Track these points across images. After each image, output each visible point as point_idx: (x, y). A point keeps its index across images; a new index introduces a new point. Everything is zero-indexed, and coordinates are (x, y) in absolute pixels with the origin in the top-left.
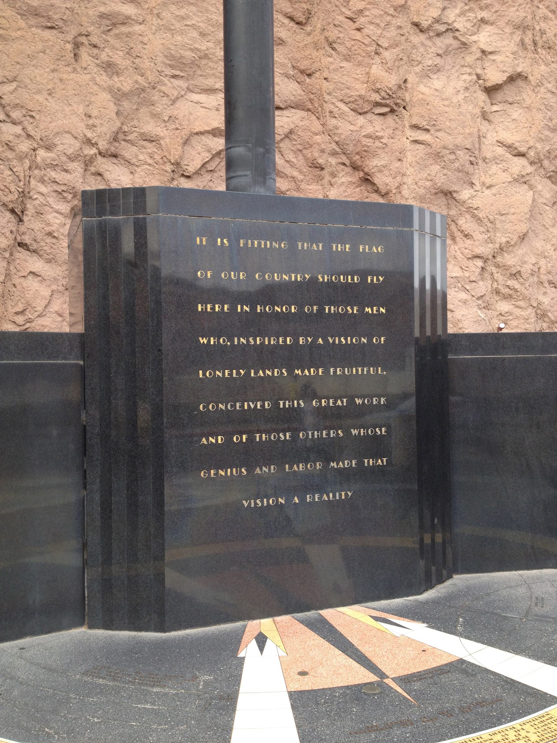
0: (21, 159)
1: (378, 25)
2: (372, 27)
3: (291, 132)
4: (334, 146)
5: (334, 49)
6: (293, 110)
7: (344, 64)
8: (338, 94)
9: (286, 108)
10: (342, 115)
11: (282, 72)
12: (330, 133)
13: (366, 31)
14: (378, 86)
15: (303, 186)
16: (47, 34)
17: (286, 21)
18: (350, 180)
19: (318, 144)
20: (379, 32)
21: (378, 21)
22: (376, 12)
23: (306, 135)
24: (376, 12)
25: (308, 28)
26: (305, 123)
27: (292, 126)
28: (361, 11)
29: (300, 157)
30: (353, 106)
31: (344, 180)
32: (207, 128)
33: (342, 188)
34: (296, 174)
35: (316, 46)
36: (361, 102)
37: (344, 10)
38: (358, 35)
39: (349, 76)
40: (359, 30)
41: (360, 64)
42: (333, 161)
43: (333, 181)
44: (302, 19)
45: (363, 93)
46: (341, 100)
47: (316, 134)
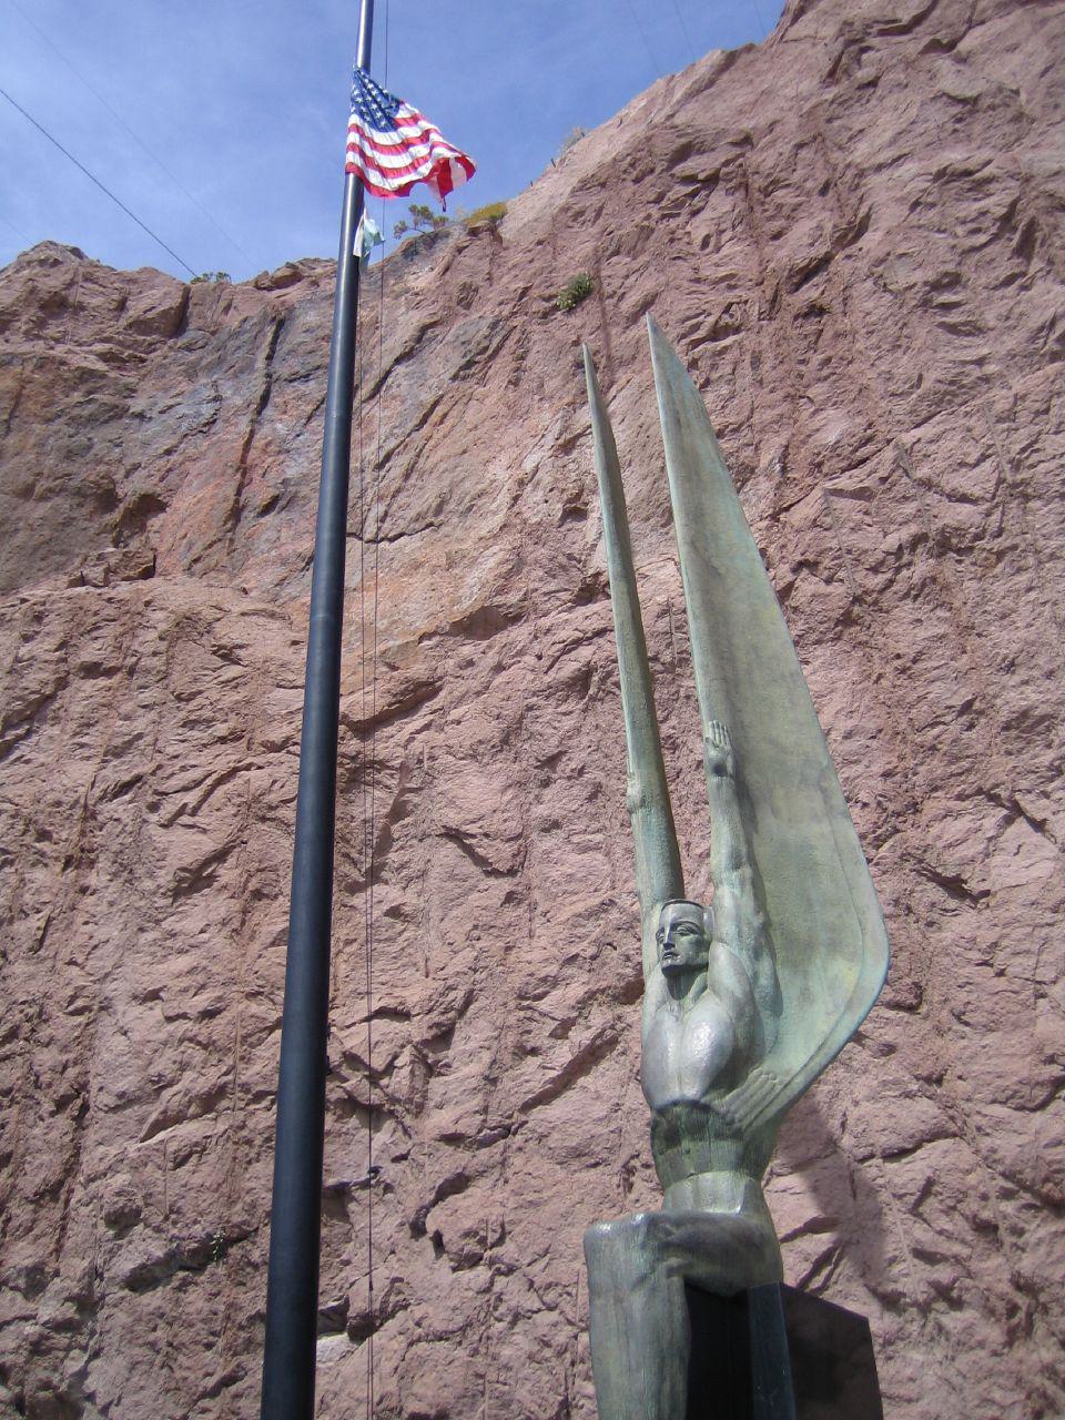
0: (560, 1354)
1: (1028, 952)
2: (1019, 960)
3: (930, 1183)
4: (1002, 1182)
5: (967, 1024)
6: (930, 1145)
7: (990, 1039)
8: (987, 1094)
9: (918, 1146)
10: (999, 1123)
11: (897, 1093)
12: (990, 1159)
13: (1010, 971)
14: (1049, 1051)
15: (974, 1265)
16: (592, 1174)
17: (891, 1014)
18: (1053, 1229)
19: (974, 1188)
20: (1032, 962)
21: (1026, 945)
22: (1019, 933)
23: (952, 1180)
24: (1019, 933)
25: (924, 1009)
26: (951, 1158)
27: (929, 1173)
28: (995, 945)
29: (957, 1216)
30: (1016, 1101)
31: (1042, 1232)
32: (798, 1225)
33: (1043, 1250)
34: (957, 1248)
35: (939, 1031)
36: (1026, 1090)
37: (970, 955)
38: (1002, 983)
39: (1000, 1055)
40: (1001, 973)
41: (1016, 1026)
42: (1008, 1207)
43: (1020, 1242)
44: (911, 1000)
45: (1025, 1073)
46: (994, 1101)
47: (968, 1172)
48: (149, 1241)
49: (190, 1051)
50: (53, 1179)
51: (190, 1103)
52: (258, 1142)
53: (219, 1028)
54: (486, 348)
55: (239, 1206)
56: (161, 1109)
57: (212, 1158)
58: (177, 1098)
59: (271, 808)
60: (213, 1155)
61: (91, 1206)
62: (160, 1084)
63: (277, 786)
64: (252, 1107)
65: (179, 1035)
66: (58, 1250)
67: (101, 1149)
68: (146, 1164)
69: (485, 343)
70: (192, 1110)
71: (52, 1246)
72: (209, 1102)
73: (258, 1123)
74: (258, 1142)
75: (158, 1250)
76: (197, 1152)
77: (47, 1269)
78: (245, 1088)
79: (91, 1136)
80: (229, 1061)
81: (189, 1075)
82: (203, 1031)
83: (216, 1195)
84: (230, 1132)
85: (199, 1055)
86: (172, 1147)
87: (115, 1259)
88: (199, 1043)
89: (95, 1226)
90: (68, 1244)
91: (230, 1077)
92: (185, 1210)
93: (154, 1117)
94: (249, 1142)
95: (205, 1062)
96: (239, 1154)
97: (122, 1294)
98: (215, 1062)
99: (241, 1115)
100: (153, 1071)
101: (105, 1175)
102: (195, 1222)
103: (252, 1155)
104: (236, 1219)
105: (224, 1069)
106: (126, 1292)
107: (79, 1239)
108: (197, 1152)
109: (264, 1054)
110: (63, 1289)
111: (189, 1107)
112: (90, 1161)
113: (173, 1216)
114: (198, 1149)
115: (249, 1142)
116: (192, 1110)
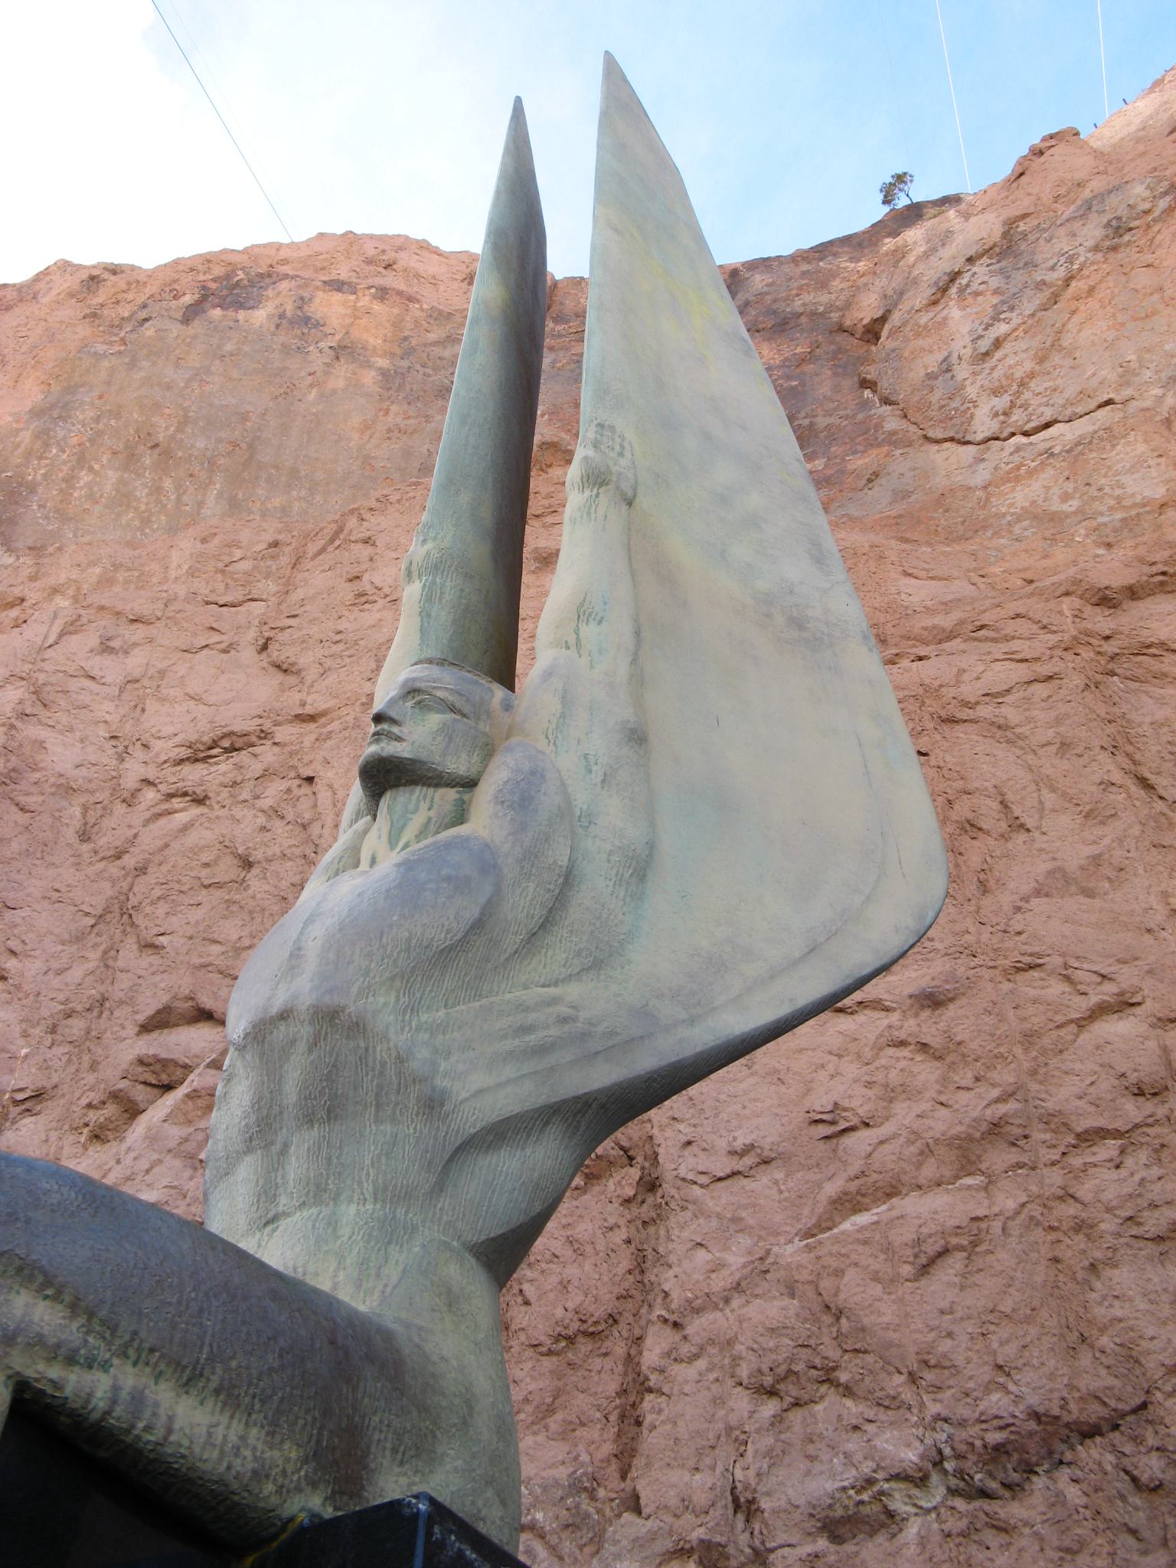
48: (870, 1428)
49: (903, 1064)
50: (599, 1312)
51: (927, 1151)
52: (1108, 1225)
53: (960, 1020)
54: (1146, 212)
55: (1085, 1359)
56: (854, 1170)
57: (1003, 1258)
58: (887, 1148)
59: (966, 704)
60: (1001, 1254)
61: (701, 1364)
62: (833, 1126)
63: (966, 677)
64: (1076, 1161)
65: (872, 1037)
66: (625, 1457)
67: (701, 1255)
68: (839, 1273)
69: (1147, 206)
70: (929, 1171)
71: (608, 1448)
72: (965, 1154)
73: (1099, 1190)
74: (1108, 1225)
75: (901, 1446)
76: (962, 1248)
77: (601, 1493)
78: (1056, 1121)
79: (680, 1233)
80: (1005, 1076)
81: (904, 1114)
82: (929, 1027)
83: (1033, 1331)
84: (1035, 1210)
85: (926, 1072)
86: (903, 1235)
87: (781, 1473)
88: (924, 1047)
89: (718, 1401)
90: (652, 1441)
91: (1012, 1106)
92: (959, 1360)
93: (831, 1189)
94: (1081, 1226)
95: (944, 1080)
96: (1066, 1254)
97: (809, 1548)
98: (968, 1081)
99: (1054, 1178)
100: (821, 1102)
101: (727, 1301)
102: (989, 1387)
103: (1098, 1255)
104: (1087, 1383)
105: (995, 1093)
106: (822, 1543)
107: (682, 1431)
108: (962, 1248)
109: (1078, 1066)
110: (653, 1536)
111: (919, 1165)
112: (684, 1272)
113: (929, 1376)
114: (967, 1242)
115: (1081, 1226)
116: (929, 1171)
